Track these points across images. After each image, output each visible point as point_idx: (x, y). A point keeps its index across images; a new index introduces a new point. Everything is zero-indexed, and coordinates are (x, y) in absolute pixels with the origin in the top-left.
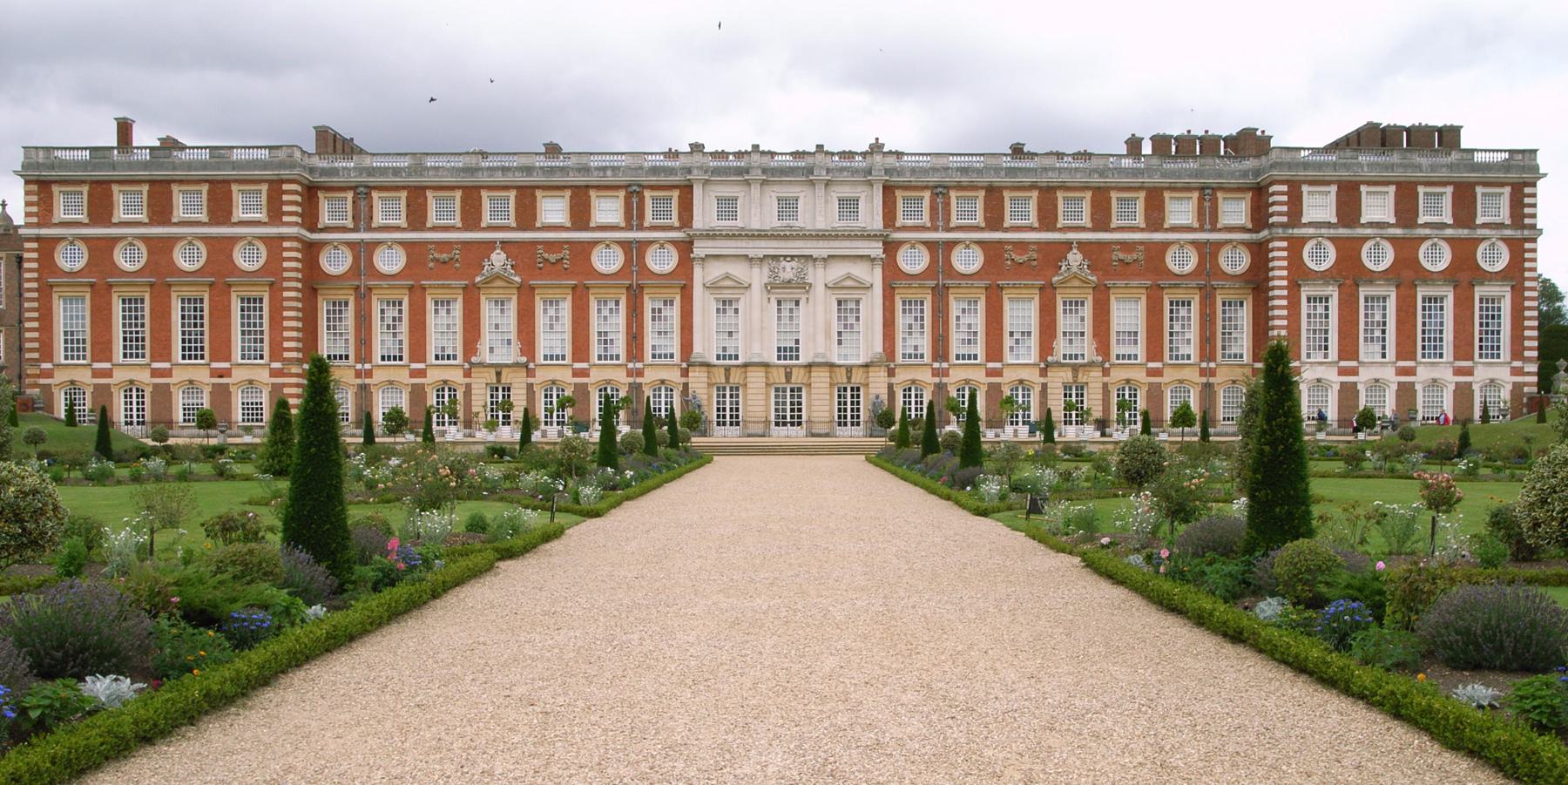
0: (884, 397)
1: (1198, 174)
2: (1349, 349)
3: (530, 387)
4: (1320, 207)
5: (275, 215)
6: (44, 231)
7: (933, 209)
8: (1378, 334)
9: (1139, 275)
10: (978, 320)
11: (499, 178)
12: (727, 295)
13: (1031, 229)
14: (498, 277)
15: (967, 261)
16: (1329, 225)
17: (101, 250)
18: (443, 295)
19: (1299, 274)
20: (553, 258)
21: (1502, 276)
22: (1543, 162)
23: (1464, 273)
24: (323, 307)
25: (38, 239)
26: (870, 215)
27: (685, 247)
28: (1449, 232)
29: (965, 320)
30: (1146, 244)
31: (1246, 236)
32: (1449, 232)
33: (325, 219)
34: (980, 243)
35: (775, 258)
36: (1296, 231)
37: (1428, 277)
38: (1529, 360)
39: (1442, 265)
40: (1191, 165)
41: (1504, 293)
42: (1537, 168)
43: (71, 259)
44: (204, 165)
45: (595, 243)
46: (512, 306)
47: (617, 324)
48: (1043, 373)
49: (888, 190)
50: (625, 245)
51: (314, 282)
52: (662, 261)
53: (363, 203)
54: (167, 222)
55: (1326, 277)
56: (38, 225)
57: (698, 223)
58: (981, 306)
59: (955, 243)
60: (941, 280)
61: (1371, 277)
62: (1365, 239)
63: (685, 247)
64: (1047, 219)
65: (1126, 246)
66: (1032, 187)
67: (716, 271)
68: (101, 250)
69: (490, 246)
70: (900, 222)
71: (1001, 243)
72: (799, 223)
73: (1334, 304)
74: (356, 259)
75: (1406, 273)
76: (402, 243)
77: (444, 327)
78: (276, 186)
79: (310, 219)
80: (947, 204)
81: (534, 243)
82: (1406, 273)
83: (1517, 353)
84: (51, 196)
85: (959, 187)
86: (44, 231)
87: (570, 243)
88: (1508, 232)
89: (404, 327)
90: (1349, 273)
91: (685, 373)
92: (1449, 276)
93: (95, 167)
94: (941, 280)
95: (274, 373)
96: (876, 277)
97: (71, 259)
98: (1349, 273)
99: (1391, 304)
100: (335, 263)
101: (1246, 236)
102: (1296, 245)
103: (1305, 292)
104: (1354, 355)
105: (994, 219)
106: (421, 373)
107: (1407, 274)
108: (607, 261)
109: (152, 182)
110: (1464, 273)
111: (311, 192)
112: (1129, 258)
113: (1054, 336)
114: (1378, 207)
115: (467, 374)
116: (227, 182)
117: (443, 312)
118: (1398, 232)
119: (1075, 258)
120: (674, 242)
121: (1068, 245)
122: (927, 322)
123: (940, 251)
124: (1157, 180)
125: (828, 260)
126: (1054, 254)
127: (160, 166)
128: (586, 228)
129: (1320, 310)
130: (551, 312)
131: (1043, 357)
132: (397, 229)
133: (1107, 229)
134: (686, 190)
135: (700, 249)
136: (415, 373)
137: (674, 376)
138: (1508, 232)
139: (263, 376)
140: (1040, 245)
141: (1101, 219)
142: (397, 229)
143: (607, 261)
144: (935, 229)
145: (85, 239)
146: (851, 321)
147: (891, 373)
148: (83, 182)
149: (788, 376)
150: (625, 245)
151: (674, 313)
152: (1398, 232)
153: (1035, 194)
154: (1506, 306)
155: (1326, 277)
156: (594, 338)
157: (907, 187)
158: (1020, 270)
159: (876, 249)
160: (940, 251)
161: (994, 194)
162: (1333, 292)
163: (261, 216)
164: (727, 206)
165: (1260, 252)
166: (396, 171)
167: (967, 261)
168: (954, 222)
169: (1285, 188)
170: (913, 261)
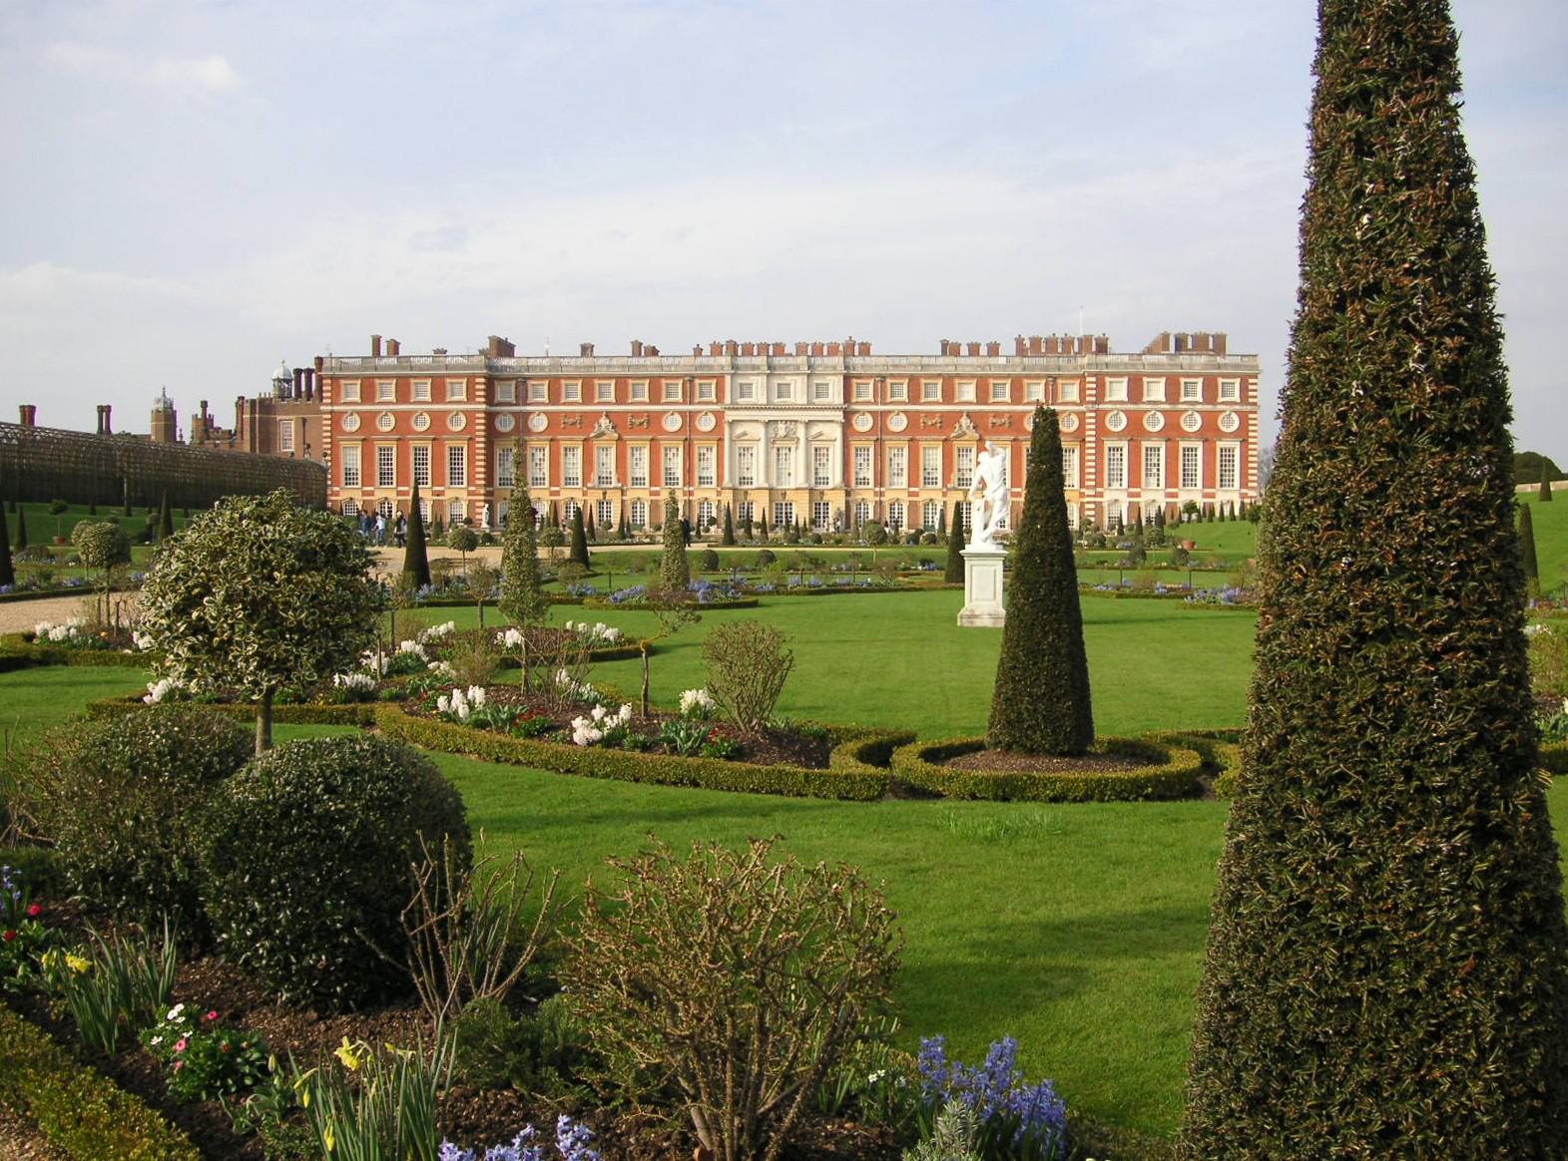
0: (843, 509)
1: (1045, 368)
2: (1134, 481)
3: (623, 502)
4: (1119, 391)
5: (471, 398)
6: (336, 408)
7: (875, 390)
8: (1155, 471)
9: (1006, 432)
10: (904, 461)
11: (604, 372)
12: (746, 444)
13: (937, 403)
14: (603, 434)
15: (898, 423)
16: (1122, 402)
17: (368, 420)
18: (568, 444)
19: (1102, 431)
20: (637, 422)
21: (1234, 435)
22: (1261, 362)
23: (1210, 432)
24: (498, 451)
25: (331, 412)
26: (835, 396)
27: (719, 415)
28: (1199, 407)
29: (895, 461)
30: (1011, 414)
31: (1076, 408)
32: (1199, 407)
33: (499, 398)
34: (905, 412)
35: (776, 421)
36: (1101, 406)
37: (1186, 436)
38: (1252, 488)
39: (1196, 428)
40: (1042, 361)
41: (1236, 445)
42: (1256, 367)
43: (352, 425)
44: (429, 368)
45: (665, 412)
46: (613, 451)
47: (677, 465)
48: (944, 494)
49: (847, 379)
50: (682, 414)
51: (492, 435)
52: (706, 424)
53: (521, 388)
54: (406, 401)
55: (1120, 435)
56: (331, 404)
57: (728, 400)
58: (906, 452)
59: (890, 412)
60: (880, 433)
61: (1149, 435)
62: (1146, 411)
63: (719, 415)
64: (948, 396)
65: (997, 414)
66: (939, 375)
67: (739, 430)
68: (368, 420)
69: (598, 414)
70: (854, 400)
71: (918, 412)
72: (791, 400)
73: (1125, 451)
74: (517, 422)
75: (1172, 432)
76: (545, 413)
77: (574, 464)
78: (471, 379)
79: (490, 399)
80: (883, 389)
81: (627, 412)
82: (1172, 432)
83: (1244, 484)
84: (339, 386)
85: (892, 376)
86: (336, 408)
87: (649, 413)
88: (1237, 407)
89: (546, 465)
90: (1135, 431)
91: (719, 493)
92: (1199, 435)
93: (366, 369)
94: (880, 433)
95: (470, 493)
96: (836, 432)
97: (352, 425)
98: (1135, 431)
99: (1162, 452)
100: (506, 425)
101: (1076, 408)
102: (1100, 416)
103: (1108, 444)
104: (1138, 485)
105: (914, 398)
106: (557, 493)
107: (1172, 434)
108: (673, 424)
109: (398, 377)
110: (1210, 432)
111: (490, 382)
112: (998, 421)
113: (951, 471)
114: (1156, 391)
115: (585, 494)
116: (442, 377)
117: (570, 455)
118: (1167, 407)
119: (965, 421)
120: (713, 412)
121: (962, 412)
122: (871, 462)
123: (880, 418)
124: (1019, 371)
125: (809, 424)
126: (949, 420)
127: (404, 368)
128: (659, 403)
129: (1117, 456)
130: (637, 455)
131: (944, 485)
132: (543, 404)
133: (986, 404)
134: (720, 378)
135: (730, 416)
136: (553, 493)
137: (712, 496)
138: (1237, 407)
139: (463, 495)
140: (943, 414)
141: (982, 396)
142: (543, 404)
143: (673, 424)
144: (875, 403)
145: (359, 413)
146: (824, 460)
147: (848, 494)
148: (357, 378)
149: (784, 495)
150: (682, 414)
151: (713, 456)
152: (1167, 407)
153: (940, 381)
154: (1237, 453)
155: (1120, 435)
156: (663, 472)
157: (859, 377)
158: (930, 430)
159: (839, 416)
160: (880, 418)
161: (913, 380)
162: (1124, 444)
163: (464, 397)
164: (744, 391)
165: (1081, 416)
166: (542, 368)
167: (898, 423)
168: (889, 400)
169: (1094, 379)
170: (864, 424)
